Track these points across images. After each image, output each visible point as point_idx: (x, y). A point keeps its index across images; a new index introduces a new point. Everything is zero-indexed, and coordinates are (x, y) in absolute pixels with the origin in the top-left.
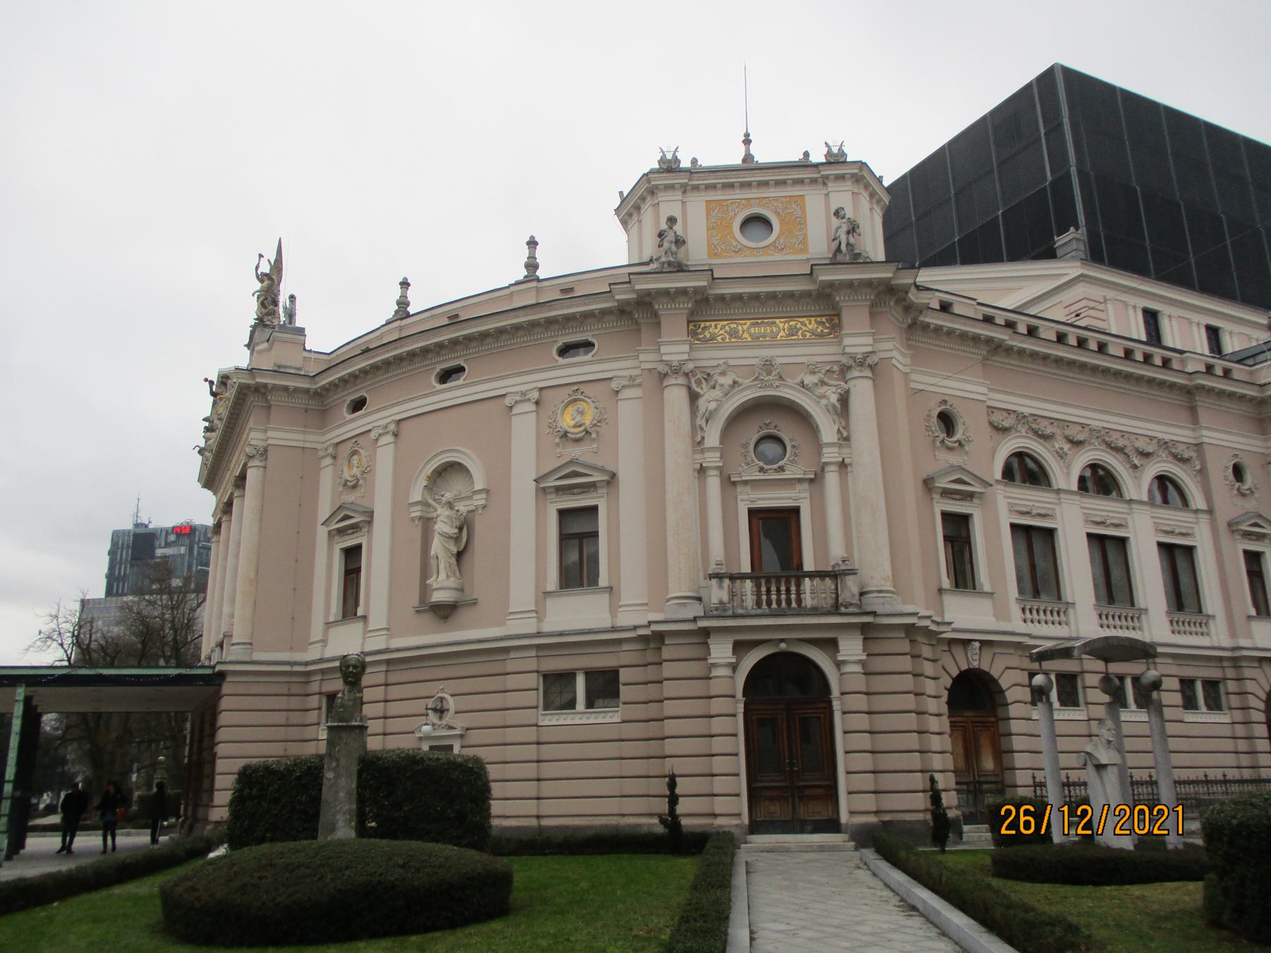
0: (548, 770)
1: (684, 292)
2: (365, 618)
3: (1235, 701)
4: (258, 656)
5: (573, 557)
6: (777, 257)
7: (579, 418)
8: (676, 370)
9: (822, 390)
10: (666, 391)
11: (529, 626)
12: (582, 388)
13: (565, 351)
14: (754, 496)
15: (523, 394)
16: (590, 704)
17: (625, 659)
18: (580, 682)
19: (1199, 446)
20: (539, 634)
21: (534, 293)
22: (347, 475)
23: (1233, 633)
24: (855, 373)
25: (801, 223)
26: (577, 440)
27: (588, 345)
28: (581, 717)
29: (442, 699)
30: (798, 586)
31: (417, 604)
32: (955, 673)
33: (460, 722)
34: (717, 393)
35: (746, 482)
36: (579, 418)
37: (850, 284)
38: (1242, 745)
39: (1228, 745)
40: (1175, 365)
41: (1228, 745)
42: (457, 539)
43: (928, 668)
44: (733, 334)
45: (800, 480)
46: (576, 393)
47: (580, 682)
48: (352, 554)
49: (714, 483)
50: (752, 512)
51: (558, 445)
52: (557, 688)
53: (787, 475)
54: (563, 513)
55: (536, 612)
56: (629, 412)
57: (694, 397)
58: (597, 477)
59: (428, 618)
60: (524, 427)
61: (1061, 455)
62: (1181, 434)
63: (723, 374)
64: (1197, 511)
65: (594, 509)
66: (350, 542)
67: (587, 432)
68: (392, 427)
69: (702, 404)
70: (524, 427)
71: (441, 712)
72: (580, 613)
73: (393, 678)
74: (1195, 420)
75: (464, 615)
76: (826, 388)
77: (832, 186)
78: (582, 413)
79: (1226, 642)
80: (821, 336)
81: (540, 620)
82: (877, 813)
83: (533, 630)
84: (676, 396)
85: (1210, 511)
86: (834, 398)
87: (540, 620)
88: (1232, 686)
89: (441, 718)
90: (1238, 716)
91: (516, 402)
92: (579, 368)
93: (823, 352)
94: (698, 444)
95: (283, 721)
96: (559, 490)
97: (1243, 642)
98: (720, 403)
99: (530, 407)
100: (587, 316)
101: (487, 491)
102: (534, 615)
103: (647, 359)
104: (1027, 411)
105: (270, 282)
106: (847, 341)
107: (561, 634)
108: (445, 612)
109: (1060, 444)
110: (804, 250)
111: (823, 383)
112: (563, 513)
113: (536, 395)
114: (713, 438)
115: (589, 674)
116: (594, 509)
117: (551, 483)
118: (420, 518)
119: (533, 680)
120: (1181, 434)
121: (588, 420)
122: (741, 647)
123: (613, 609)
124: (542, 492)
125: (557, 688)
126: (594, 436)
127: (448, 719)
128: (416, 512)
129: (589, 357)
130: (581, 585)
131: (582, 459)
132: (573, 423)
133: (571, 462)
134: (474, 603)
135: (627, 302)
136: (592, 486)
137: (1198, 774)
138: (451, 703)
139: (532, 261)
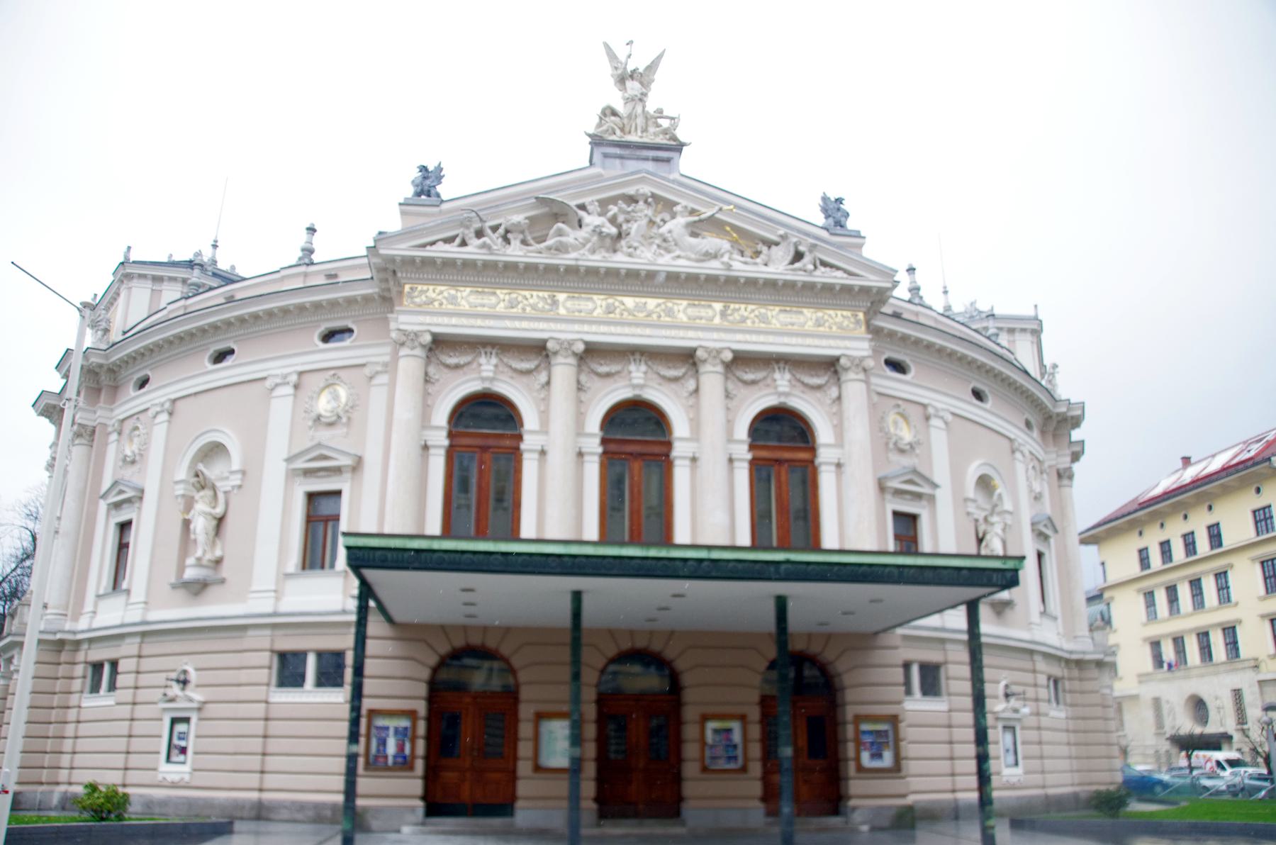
11: (266, 605)
12: (341, 373)
15: (285, 377)
18: (311, 662)
20: (275, 614)
21: (301, 279)
22: (128, 452)
26: (331, 424)
27: (350, 331)
29: (185, 672)
33: (198, 696)
46: (334, 374)
47: (311, 662)
48: (124, 527)
51: (310, 428)
54: (312, 497)
55: (275, 591)
58: (344, 461)
59: (181, 593)
60: (282, 407)
65: (338, 493)
66: (123, 517)
67: (339, 417)
68: (167, 405)
70: (282, 407)
71: (184, 683)
73: (147, 650)
75: (213, 591)
81: (277, 599)
83: (269, 610)
87: (277, 599)
89: (183, 689)
91: (277, 385)
92: (337, 353)
96: (308, 473)
99: (289, 390)
100: (350, 301)
101: (244, 473)
102: (273, 594)
108: (197, 588)
112: (312, 497)
115: (320, 654)
116: (338, 493)
117: (301, 464)
118: (183, 496)
124: (293, 474)
125: (289, 670)
126: (344, 420)
128: (180, 490)
129: (347, 342)
130: (323, 567)
131: (325, 443)
133: (319, 445)
134: (223, 581)
136: (337, 470)
138: (193, 676)
139: (308, 246)
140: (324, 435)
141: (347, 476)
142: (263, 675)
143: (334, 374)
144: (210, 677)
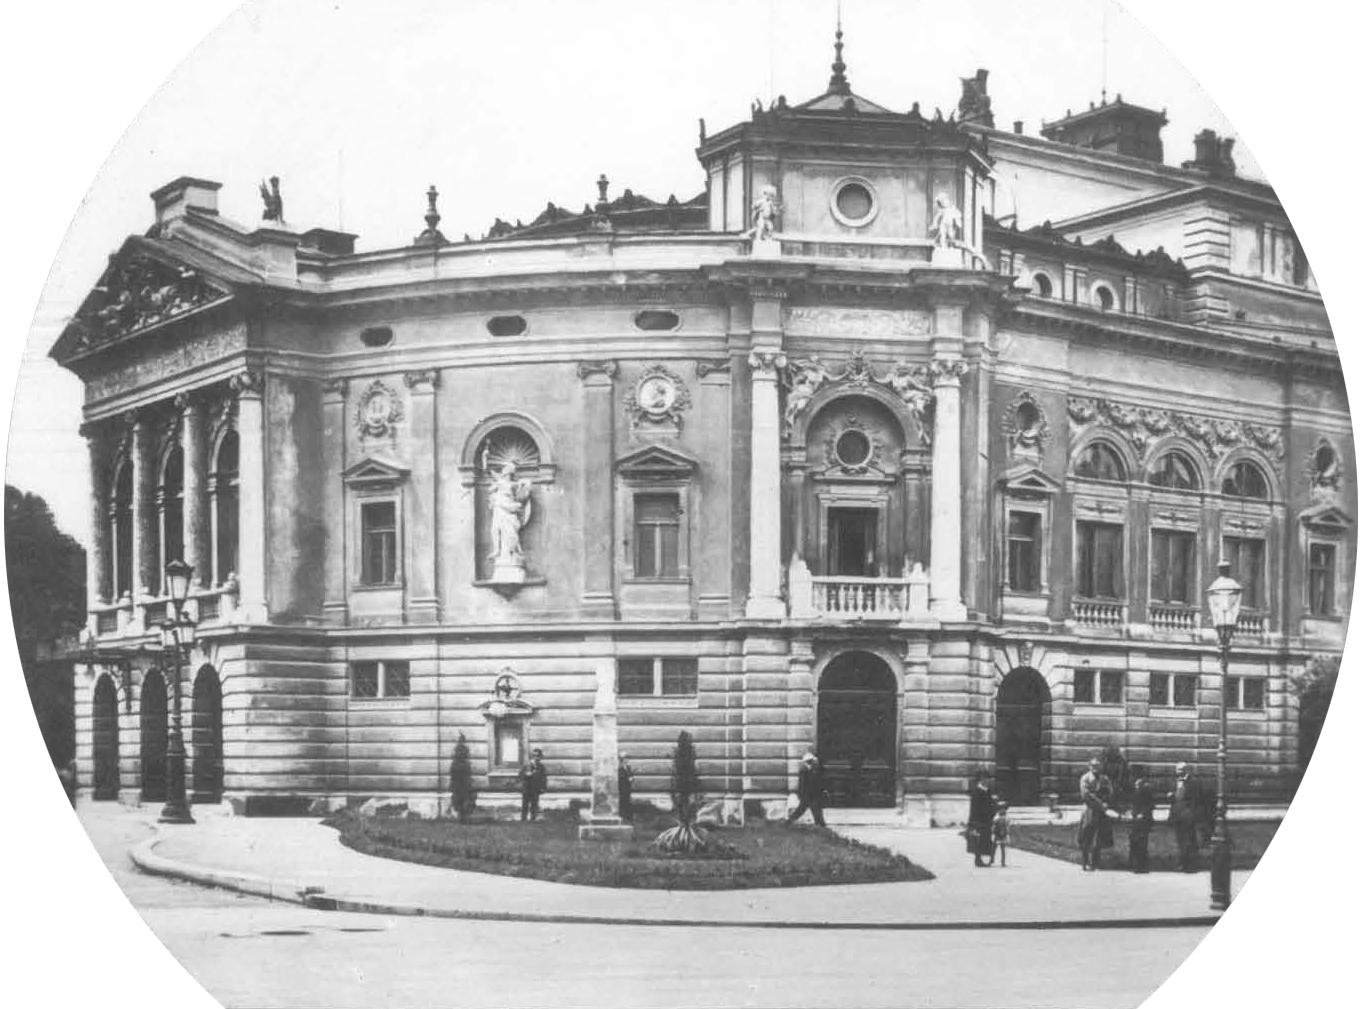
7: (660, 398)
9: (910, 394)
10: (756, 385)
12: (664, 364)
15: (598, 363)
24: (942, 381)
26: (657, 422)
32: (1006, 670)
42: (519, 514)
43: (985, 668)
76: (914, 392)
78: (663, 392)
86: (920, 405)
111: (912, 387)
121: (669, 400)
132: (653, 402)
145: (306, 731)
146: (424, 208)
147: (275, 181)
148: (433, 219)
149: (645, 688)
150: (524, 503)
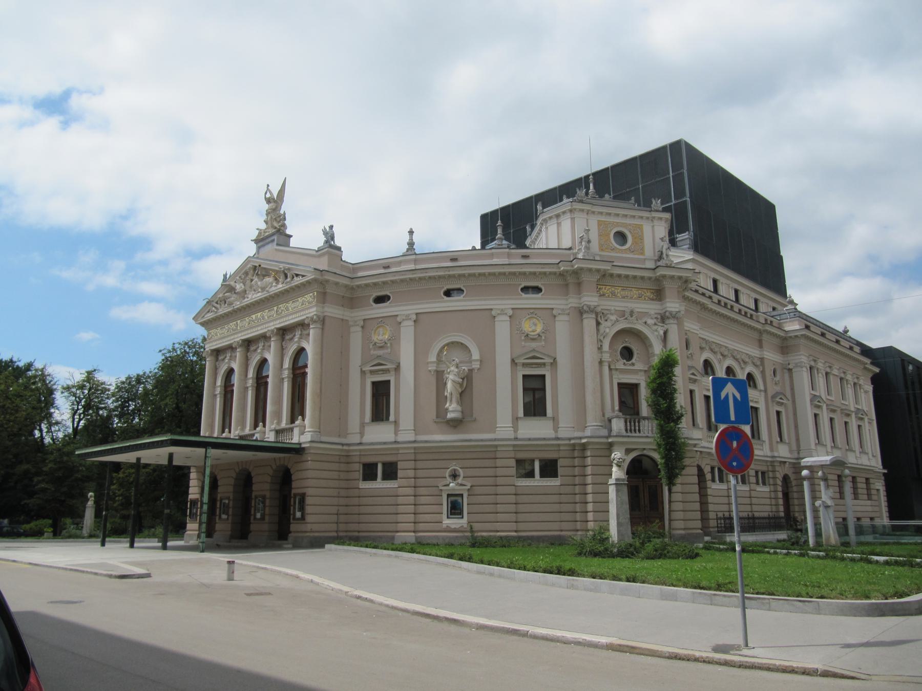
0: (521, 508)
1: (598, 271)
2: (396, 423)
3: (771, 481)
4: (324, 439)
5: (530, 398)
6: (631, 256)
7: (533, 328)
8: (592, 310)
9: (656, 327)
10: (585, 321)
12: (536, 312)
13: (525, 289)
14: (621, 376)
16: (542, 476)
17: (562, 454)
19: (762, 359)
23: (772, 450)
25: (642, 238)
26: (533, 339)
28: (537, 481)
30: (639, 422)
31: (435, 417)
34: (609, 324)
35: (617, 369)
36: (533, 328)
37: (672, 277)
38: (773, 502)
39: (768, 501)
40: (754, 318)
41: (768, 501)
42: (461, 385)
44: (613, 294)
45: (641, 370)
49: (606, 369)
50: (619, 384)
52: (524, 469)
53: (635, 367)
54: (525, 377)
56: (562, 328)
57: (598, 324)
58: (548, 360)
60: (503, 329)
61: (720, 362)
62: (755, 352)
63: (612, 314)
64: (761, 391)
68: (414, 317)
69: (601, 327)
72: (535, 430)
74: (761, 346)
77: (656, 222)
78: (535, 325)
79: (769, 454)
80: (652, 299)
82: (684, 529)
84: (589, 323)
85: (765, 391)
86: (662, 333)
88: (771, 475)
90: (772, 488)
93: (653, 308)
94: (600, 348)
95: (336, 477)
97: (776, 454)
98: (610, 329)
103: (573, 301)
104: (711, 340)
105: (275, 203)
106: (668, 305)
107: (530, 439)
108: (456, 424)
109: (719, 356)
110: (642, 253)
112: (525, 377)
113: (510, 312)
114: (606, 347)
115: (541, 461)
119: (513, 463)
120: (755, 352)
121: (539, 329)
122: (628, 451)
123: (556, 428)
127: (460, 480)
128: (432, 368)
133: (534, 350)
135: (567, 271)
137: (766, 515)
140: (534, 345)
141: (548, 367)
142: (513, 471)
143: (533, 312)
144: (471, 472)
145: (355, 501)
146: (407, 238)
147: (331, 227)
148: (411, 244)
149: (531, 475)
150: (463, 379)
